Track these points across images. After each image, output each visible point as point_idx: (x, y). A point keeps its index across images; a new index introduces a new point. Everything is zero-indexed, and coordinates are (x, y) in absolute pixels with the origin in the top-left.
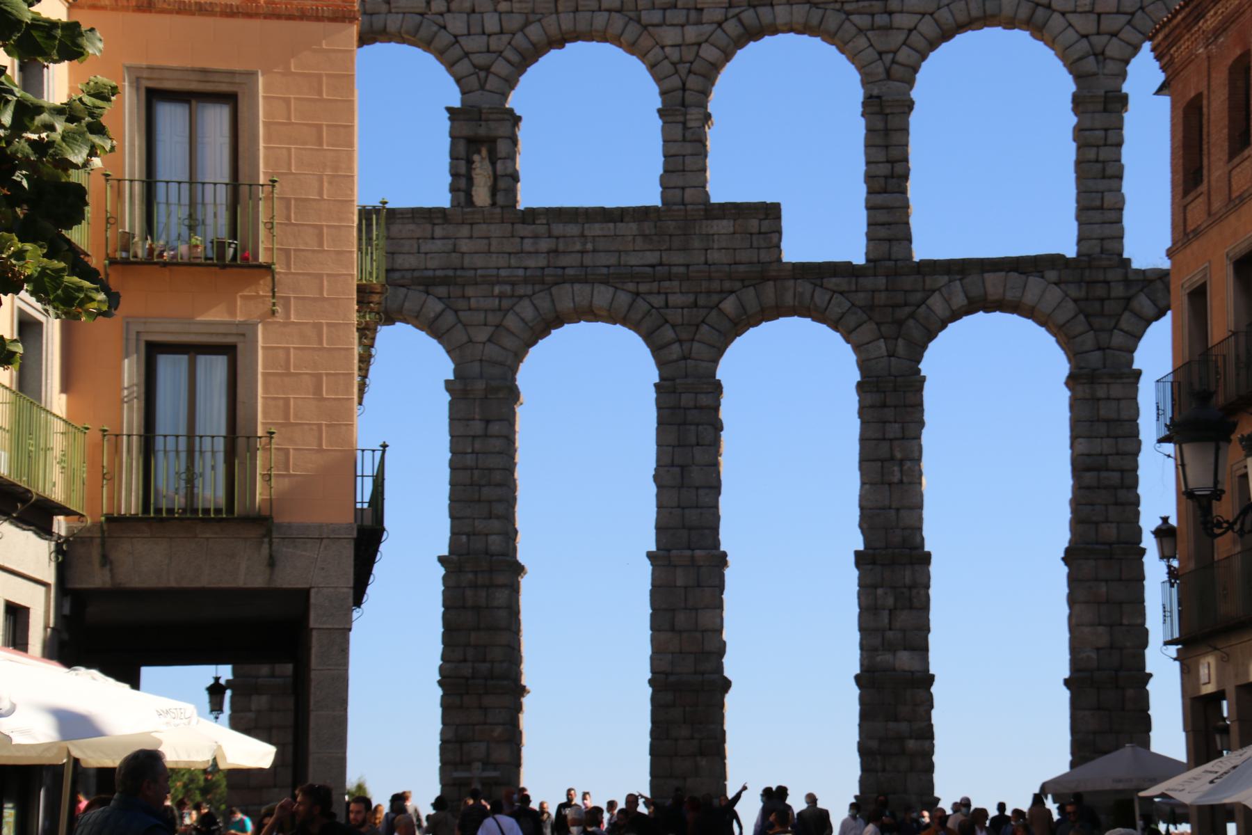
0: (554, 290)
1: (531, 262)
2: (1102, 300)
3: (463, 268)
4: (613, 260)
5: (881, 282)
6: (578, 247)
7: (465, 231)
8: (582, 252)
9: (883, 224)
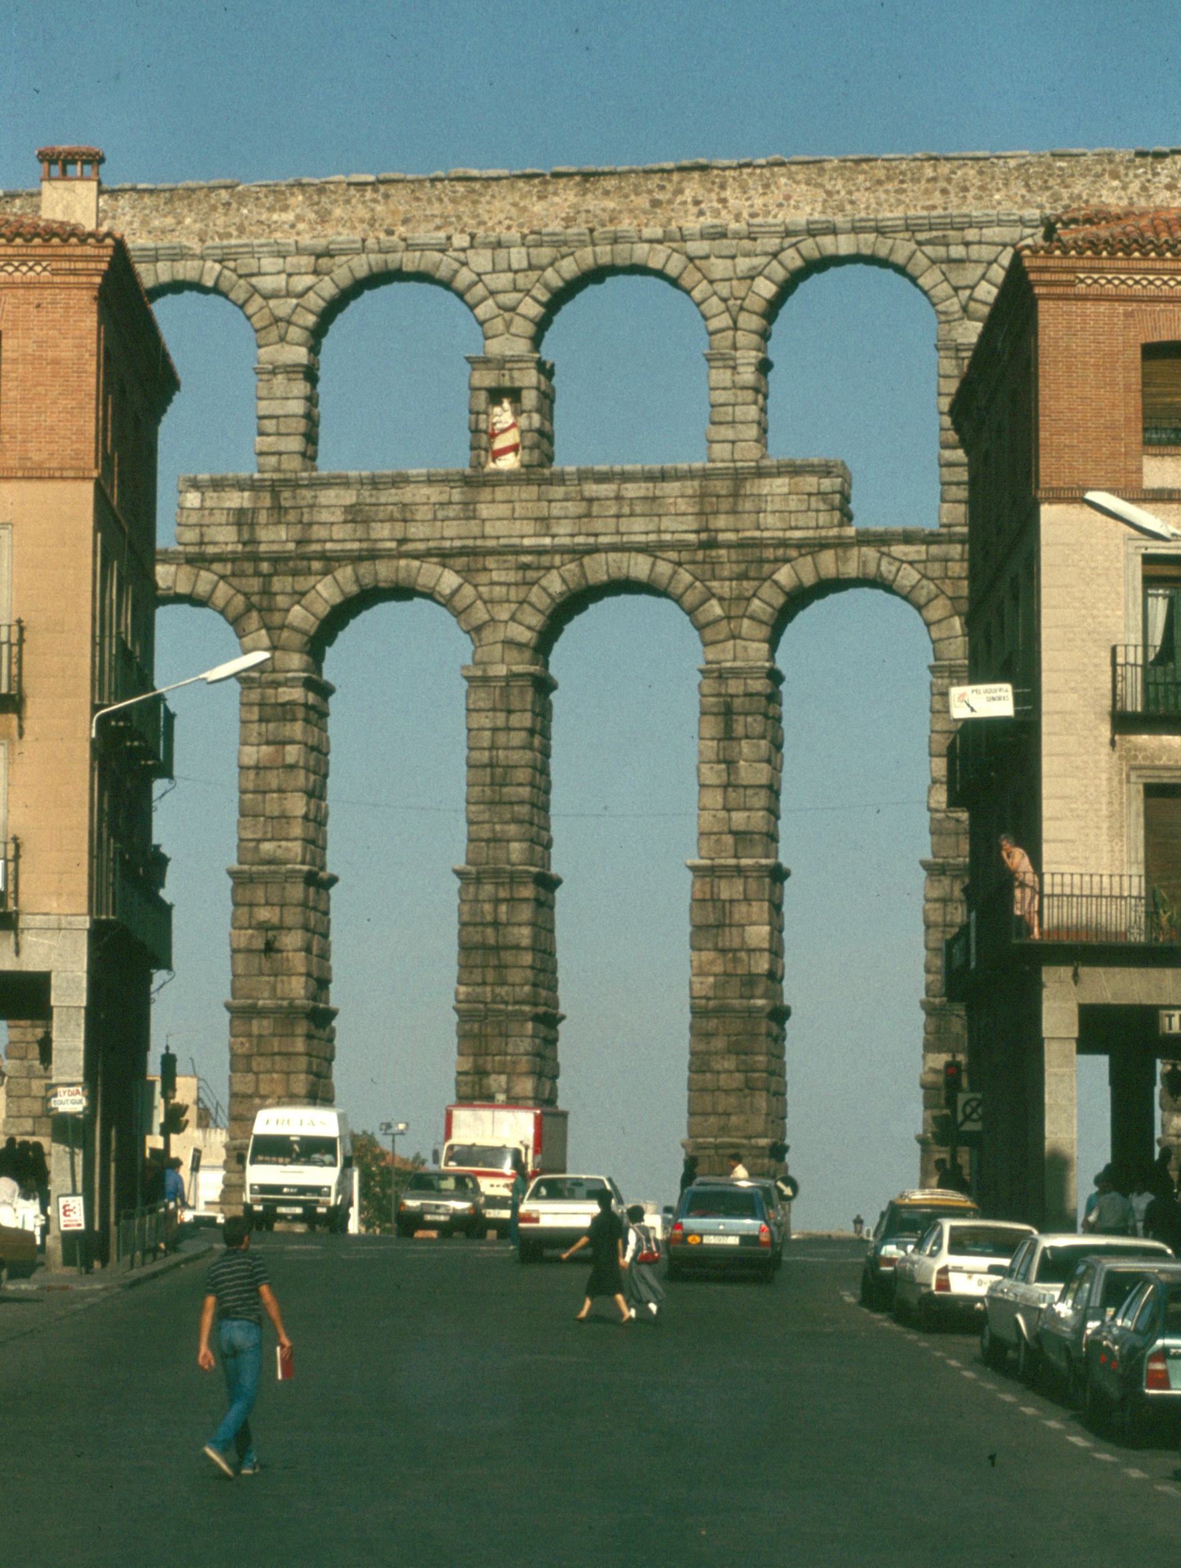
3: (483, 537)
6: (613, 511)
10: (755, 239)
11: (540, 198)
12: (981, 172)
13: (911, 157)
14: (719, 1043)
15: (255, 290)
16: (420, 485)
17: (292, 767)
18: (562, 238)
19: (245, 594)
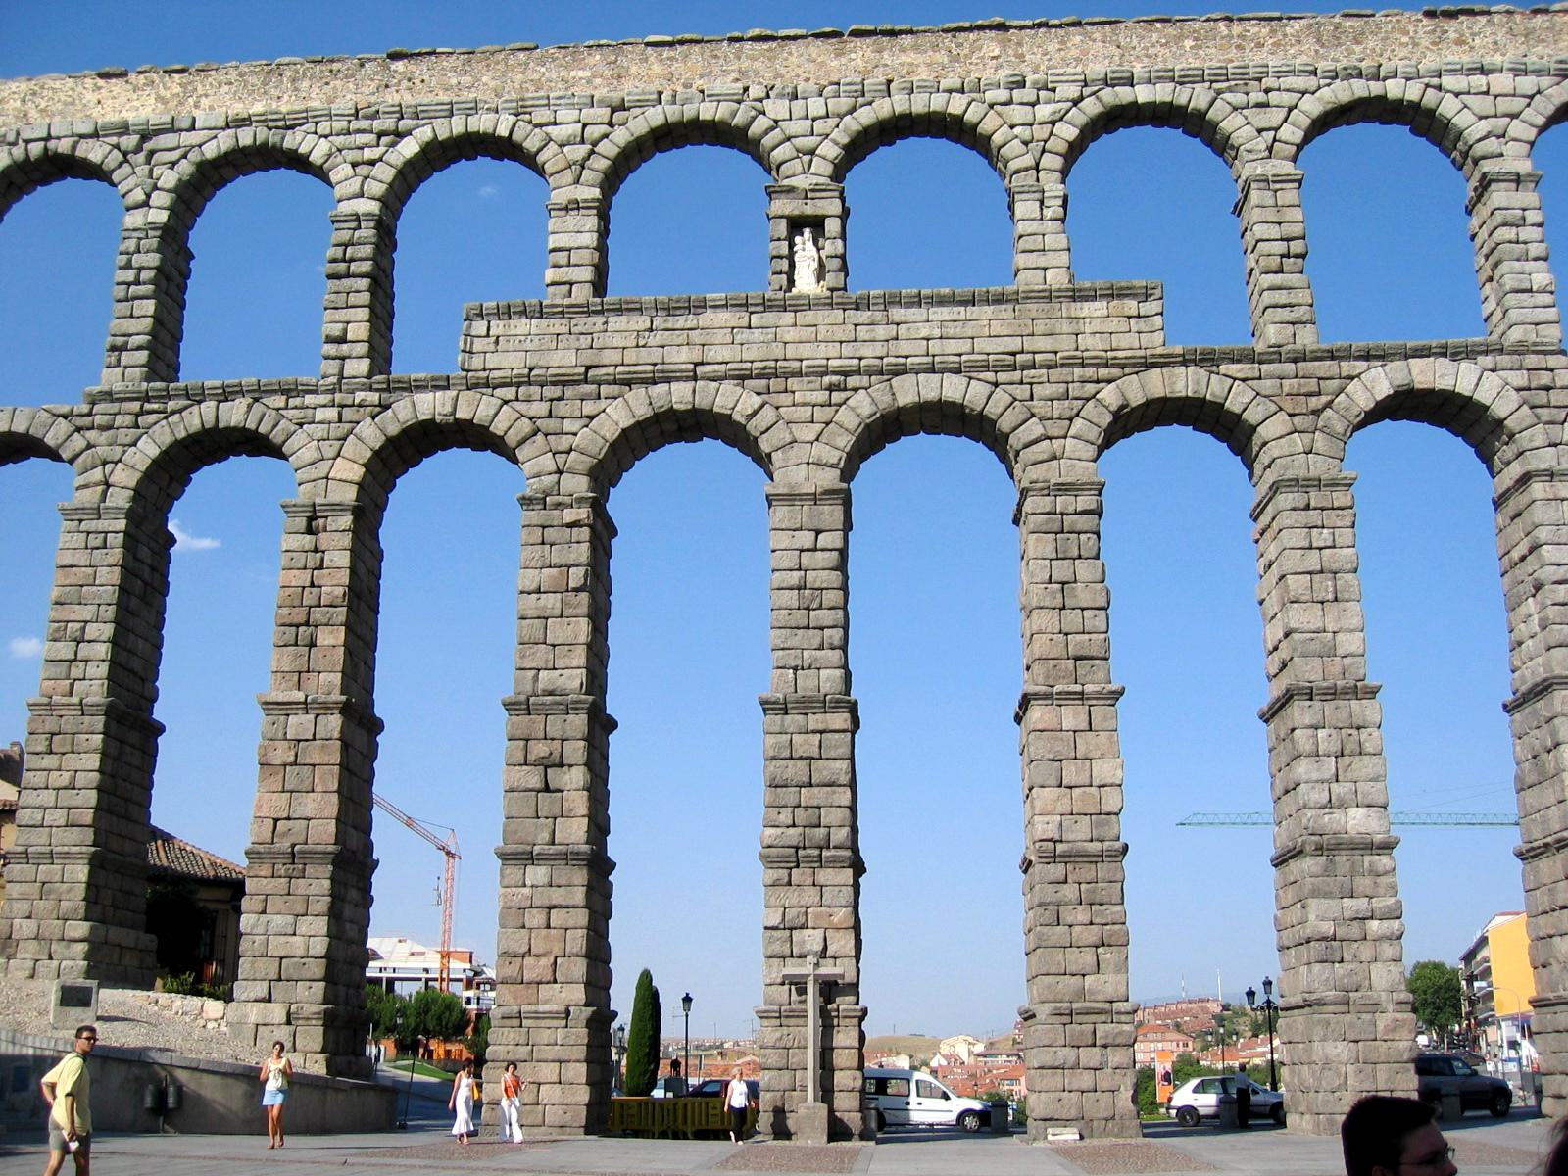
0: (895, 381)
1: (867, 350)
2: (1548, 389)
4: (965, 346)
6: (924, 333)
9: (1284, 306)
10: (1054, 90)
11: (838, 55)
12: (1273, 32)
13: (1204, 18)
14: (1069, 891)
16: (718, 310)
17: (577, 590)
19: (531, 419)
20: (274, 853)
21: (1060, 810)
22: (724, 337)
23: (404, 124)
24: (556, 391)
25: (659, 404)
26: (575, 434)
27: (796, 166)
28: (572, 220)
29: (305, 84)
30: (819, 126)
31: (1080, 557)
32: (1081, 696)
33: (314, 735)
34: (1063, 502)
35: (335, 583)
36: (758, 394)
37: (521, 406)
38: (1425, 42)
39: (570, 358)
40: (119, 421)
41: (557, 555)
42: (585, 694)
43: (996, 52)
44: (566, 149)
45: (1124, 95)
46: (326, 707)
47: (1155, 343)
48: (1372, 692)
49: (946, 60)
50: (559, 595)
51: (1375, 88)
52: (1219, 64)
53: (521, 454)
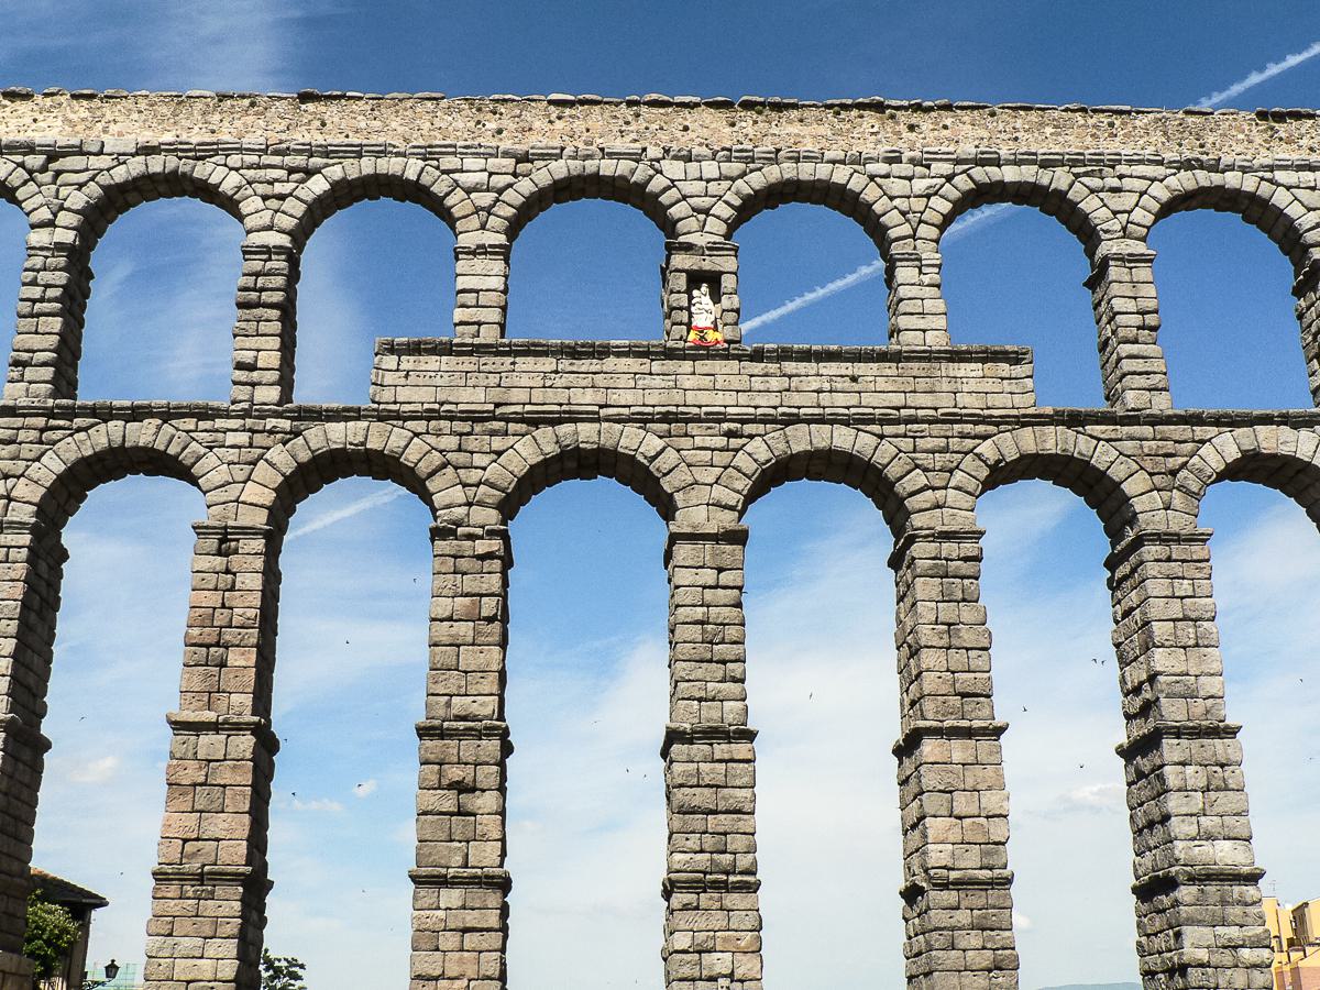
1: (761, 400)
4: (853, 399)
5: (1147, 430)
6: (815, 386)
7: (687, 366)
8: (818, 392)
9: (1140, 374)
10: (928, 167)
13: (1063, 108)
14: (963, 917)
15: (457, 184)
18: (751, 154)
19: (441, 452)
20: (183, 874)
21: (952, 840)
22: (632, 385)
23: (316, 161)
24: (465, 427)
25: (564, 443)
26: (484, 469)
27: (692, 223)
28: (480, 264)
29: (217, 117)
30: (713, 187)
31: (964, 600)
32: (968, 733)
33: (225, 755)
34: (949, 548)
35: (247, 606)
36: (660, 437)
37: (431, 439)
38: (1258, 140)
39: (480, 395)
40: (22, 435)
41: (469, 583)
42: (497, 720)
43: (875, 130)
44: (473, 195)
45: (994, 173)
46: (238, 727)
47: (1025, 403)
48: (1232, 732)
49: (829, 133)
50: (471, 624)
51: (1216, 179)
52: (1078, 151)
53: (431, 485)
